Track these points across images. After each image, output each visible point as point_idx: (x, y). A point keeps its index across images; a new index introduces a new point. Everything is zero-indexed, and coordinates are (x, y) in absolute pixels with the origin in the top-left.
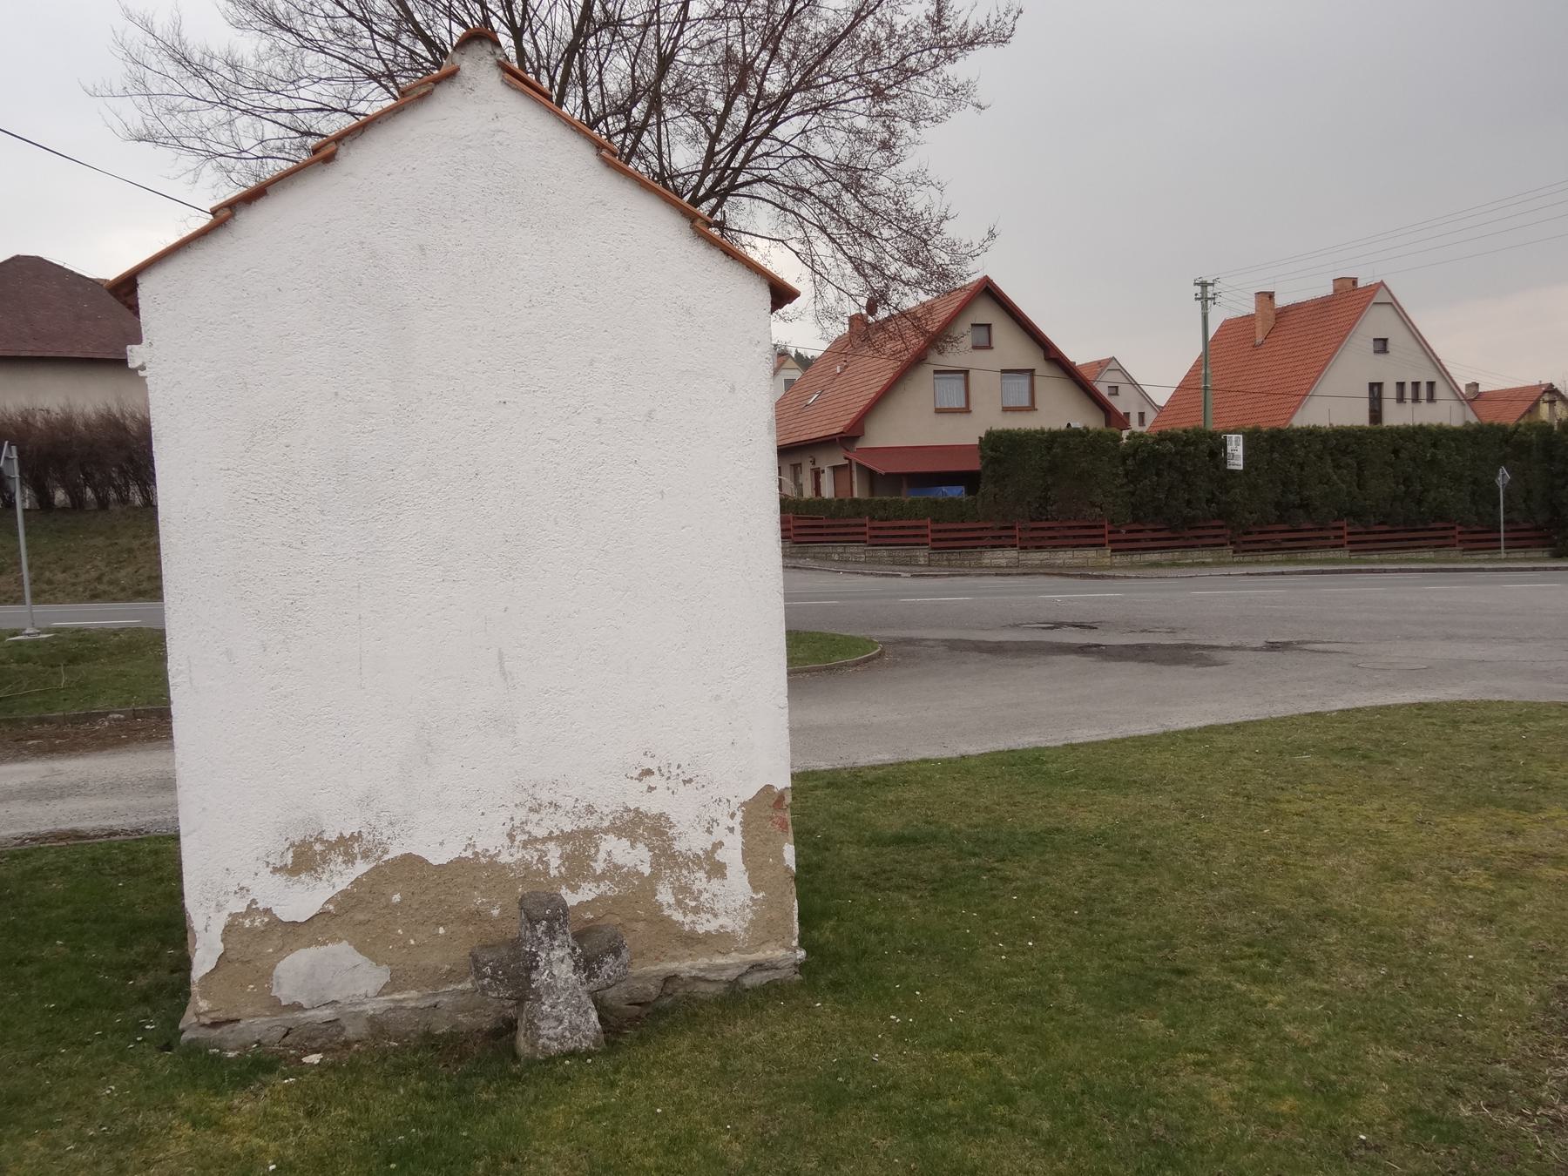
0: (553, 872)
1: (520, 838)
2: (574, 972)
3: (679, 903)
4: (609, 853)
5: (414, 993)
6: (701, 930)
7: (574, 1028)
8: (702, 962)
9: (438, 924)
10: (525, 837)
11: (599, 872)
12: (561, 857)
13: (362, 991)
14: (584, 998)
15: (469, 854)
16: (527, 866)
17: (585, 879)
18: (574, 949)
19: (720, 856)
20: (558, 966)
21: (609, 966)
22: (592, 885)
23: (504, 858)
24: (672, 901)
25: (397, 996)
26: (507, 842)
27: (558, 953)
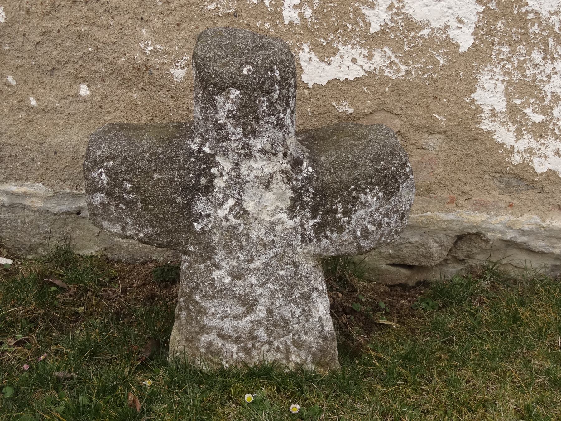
2: (291, 211)
3: (513, 113)
5: (39, 188)
6: (540, 166)
7: (277, 325)
8: (529, 220)
9: (78, 79)
11: (375, 28)
14: (307, 267)
18: (296, 163)
20: (256, 194)
21: (368, 213)
22: (358, 52)
24: (501, 106)
25: (13, 188)
27: (260, 166)
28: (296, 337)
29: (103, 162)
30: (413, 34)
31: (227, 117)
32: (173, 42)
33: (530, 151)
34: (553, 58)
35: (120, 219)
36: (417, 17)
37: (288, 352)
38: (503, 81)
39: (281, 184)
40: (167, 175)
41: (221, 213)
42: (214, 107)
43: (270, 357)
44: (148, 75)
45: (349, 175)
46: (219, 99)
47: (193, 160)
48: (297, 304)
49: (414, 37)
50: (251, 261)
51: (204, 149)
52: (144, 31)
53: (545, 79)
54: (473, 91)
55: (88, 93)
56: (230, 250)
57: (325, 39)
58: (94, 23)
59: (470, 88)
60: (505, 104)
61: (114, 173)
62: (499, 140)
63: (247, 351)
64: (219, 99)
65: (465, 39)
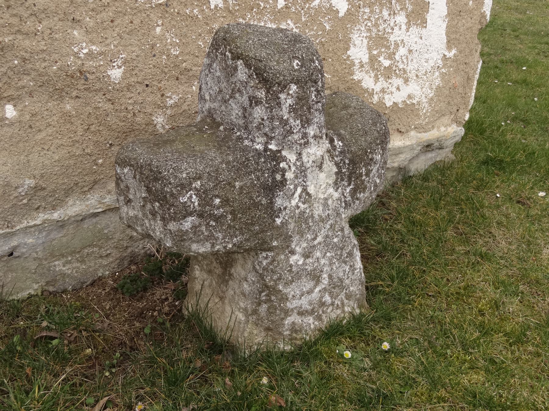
2: (336, 185)
7: (336, 285)
24: (366, 59)
27: (316, 151)
28: (347, 292)
29: (191, 184)
30: (308, 5)
31: (290, 112)
32: (108, 41)
33: (383, 91)
34: (394, 13)
35: (210, 237)
38: (366, 37)
39: (329, 163)
40: (247, 181)
41: (294, 203)
42: (279, 104)
44: (83, 82)
45: (366, 141)
46: (282, 96)
47: (263, 160)
48: (345, 262)
49: (308, 9)
50: (315, 239)
51: (270, 147)
52: (75, 33)
53: (390, 31)
54: (348, 49)
55: (15, 113)
56: (301, 234)
57: (243, 19)
58: (19, 31)
59: (346, 46)
60: (367, 56)
61: (204, 193)
62: (365, 86)
64: (282, 96)
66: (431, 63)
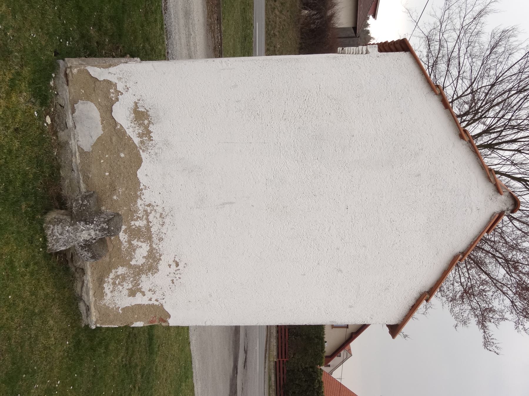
0: (133, 223)
1: (149, 209)
2: (84, 240)
3: (118, 276)
4: (141, 247)
6: (105, 285)
7: (57, 240)
8: (90, 285)
9: (110, 172)
10: (149, 211)
11: (132, 242)
12: (140, 226)
13: (80, 139)
14: (72, 244)
15: (142, 187)
16: (136, 212)
17: (129, 236)
18: (95, 239)
19: (139, 295)
20: (86, 233)
21: (85, 254)
22: (126, 239)
23: (139, 202)
24: (118, 273)
25: (77, 154)
26: (147, 203)
27: (93, 233)
33: (109, 282)
35: (76, 207)
36: (136, 251)
37: (51, 243)
43: (49, 240)
56: (73, 229)
63: (50, 235)
65: (133, 263)
66: (117, 302)
